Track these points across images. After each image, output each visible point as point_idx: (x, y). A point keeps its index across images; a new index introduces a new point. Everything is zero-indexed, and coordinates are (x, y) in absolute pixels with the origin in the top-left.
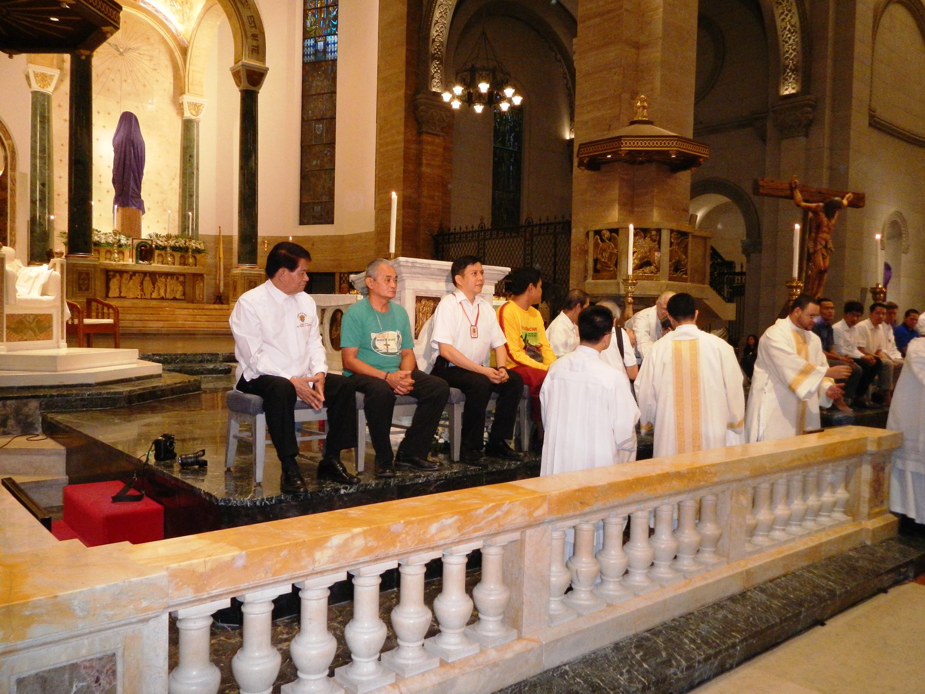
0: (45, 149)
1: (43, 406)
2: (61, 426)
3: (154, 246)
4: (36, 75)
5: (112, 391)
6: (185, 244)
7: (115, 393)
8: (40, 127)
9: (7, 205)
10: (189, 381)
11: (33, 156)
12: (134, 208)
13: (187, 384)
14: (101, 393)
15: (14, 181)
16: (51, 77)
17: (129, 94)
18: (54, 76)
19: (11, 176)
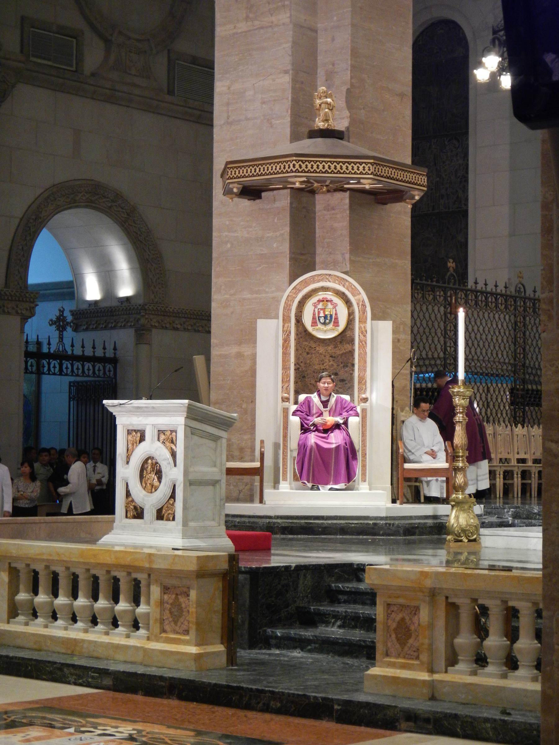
15: (363, 332)
19: (360, 328)
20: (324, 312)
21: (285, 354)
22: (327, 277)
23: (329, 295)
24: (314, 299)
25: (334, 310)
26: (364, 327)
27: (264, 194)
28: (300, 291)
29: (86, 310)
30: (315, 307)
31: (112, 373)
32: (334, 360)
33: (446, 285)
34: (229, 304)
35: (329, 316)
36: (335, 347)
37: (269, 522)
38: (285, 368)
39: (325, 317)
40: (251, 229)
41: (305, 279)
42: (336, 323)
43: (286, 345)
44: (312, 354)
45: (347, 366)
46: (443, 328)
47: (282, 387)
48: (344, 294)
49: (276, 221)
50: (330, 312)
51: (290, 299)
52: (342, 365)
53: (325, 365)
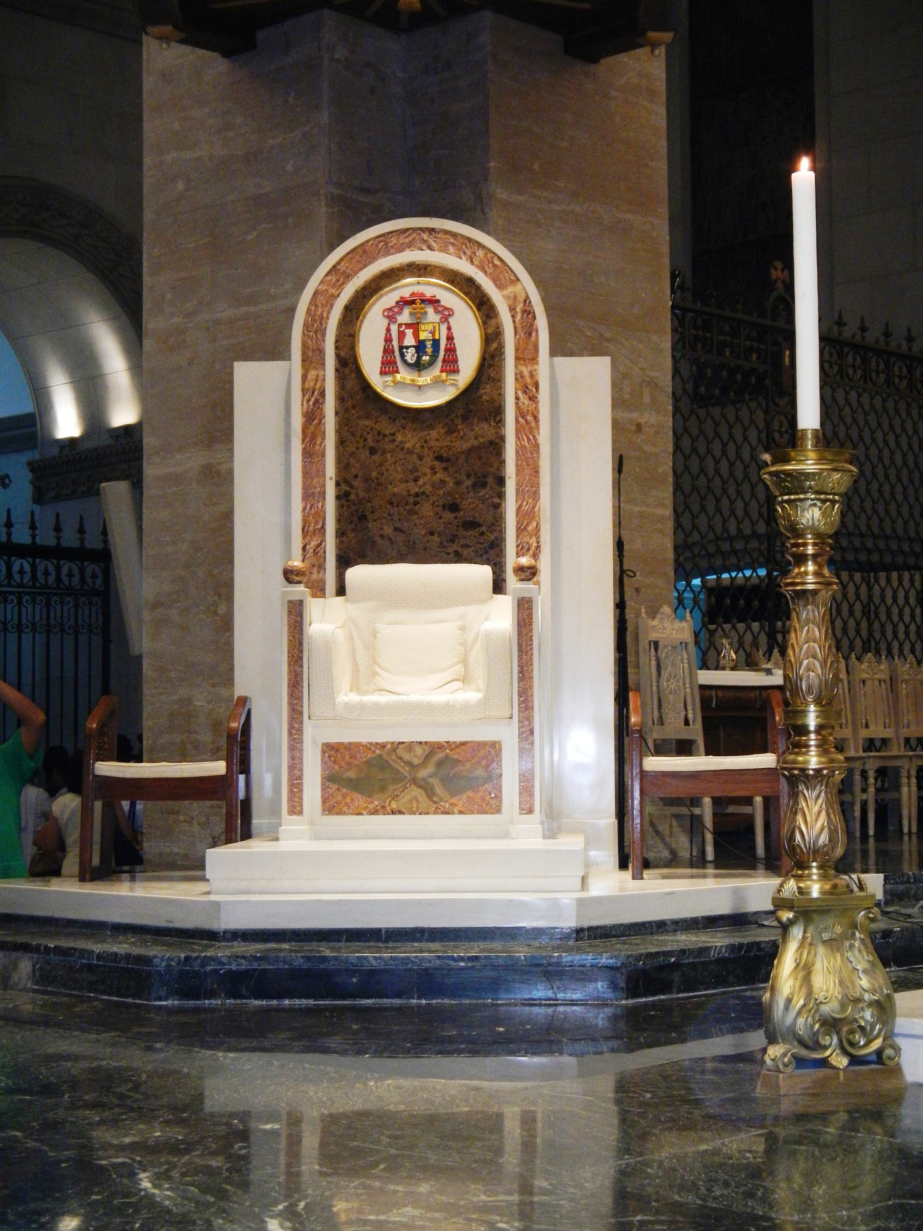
15: (529, 389)
19: (519, 377)
20: (416, 335)
21: (312, 454)
22: (425, 236)
23: (432, 287)
24: (388, 298)
25: (444, 328)
26: (532, 375)
27: (261, 35)
28: (348, 277)
29: (54, 458)
31: (99, 582)
32: (445, 469)
33: (768, 322)
34: (184, 341)
35: (429, 344)
36: (450, 432)
37: (187, 958)
38: (312, 494)
39: (420, 347)
40: (231, 134)
41: (363, 245)
42: (451, 364)
43: (312, 428)
44: (384, 452)
45: (484, 485)
46: (761, 425)
47: (304, 548)
48: (470, 281)
49: (291, 99)
50: (433, 333)
52: (469, 483)
53: (421, 482)
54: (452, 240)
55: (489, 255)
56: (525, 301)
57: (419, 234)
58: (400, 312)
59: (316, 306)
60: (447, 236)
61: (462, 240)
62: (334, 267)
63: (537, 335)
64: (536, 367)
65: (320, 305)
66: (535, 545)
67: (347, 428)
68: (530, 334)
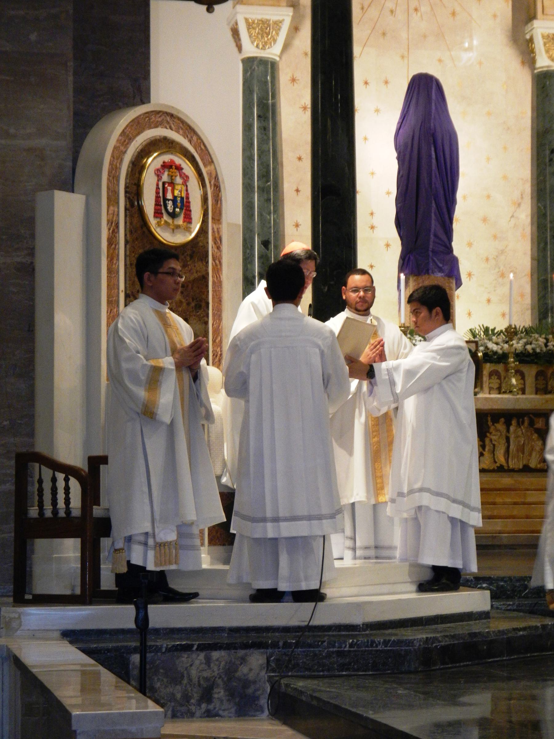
0: (268, 172)
1: (273, 665)
2: (304, 698)
3: (480, 354)
4: (250, 25)
5: (393, 638)
6: (546, 345)
7: (399, 643)
8: (259, 128)
9: (207, 286)
10: (544, 627)
11: (248, 188)
12: (440, 275)
13: (540, 631)
14: (373, 642)
15: (218, 241)
16: (278, 24)
17: (425, 36)
18: (281, 22)
19: (213, 232)
20: (173, 192)
22: (168, 119)
26: (218, 232)
30: (159, 177)
35: (179, 199)
39: (174, 200)
42: (188, 218)
51: (118, 155)
52: (193, 304)
54: (181, 125)
55: (199, 141)
56: (215, 179)
57: (165, 117)
58: (163, 174)
59: (114, 158)
60: (179, 122)
61: (186, 127)
62: (123, 131)
63: (221, 203)
64: (220, 226)
65: (115, 157)
66: (219, 353)
67: (133, 255)
68: (218, 202)
